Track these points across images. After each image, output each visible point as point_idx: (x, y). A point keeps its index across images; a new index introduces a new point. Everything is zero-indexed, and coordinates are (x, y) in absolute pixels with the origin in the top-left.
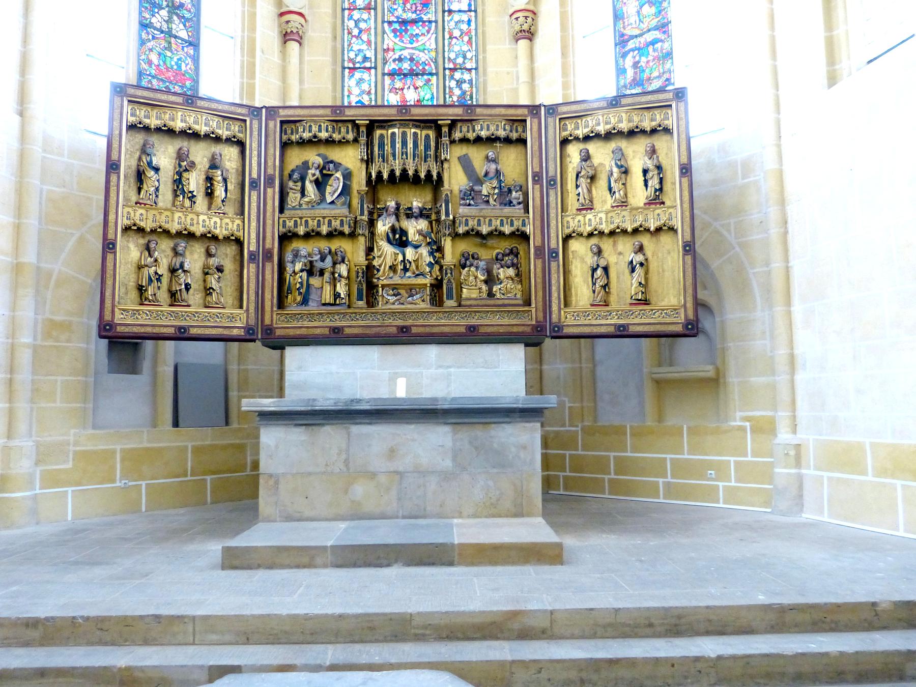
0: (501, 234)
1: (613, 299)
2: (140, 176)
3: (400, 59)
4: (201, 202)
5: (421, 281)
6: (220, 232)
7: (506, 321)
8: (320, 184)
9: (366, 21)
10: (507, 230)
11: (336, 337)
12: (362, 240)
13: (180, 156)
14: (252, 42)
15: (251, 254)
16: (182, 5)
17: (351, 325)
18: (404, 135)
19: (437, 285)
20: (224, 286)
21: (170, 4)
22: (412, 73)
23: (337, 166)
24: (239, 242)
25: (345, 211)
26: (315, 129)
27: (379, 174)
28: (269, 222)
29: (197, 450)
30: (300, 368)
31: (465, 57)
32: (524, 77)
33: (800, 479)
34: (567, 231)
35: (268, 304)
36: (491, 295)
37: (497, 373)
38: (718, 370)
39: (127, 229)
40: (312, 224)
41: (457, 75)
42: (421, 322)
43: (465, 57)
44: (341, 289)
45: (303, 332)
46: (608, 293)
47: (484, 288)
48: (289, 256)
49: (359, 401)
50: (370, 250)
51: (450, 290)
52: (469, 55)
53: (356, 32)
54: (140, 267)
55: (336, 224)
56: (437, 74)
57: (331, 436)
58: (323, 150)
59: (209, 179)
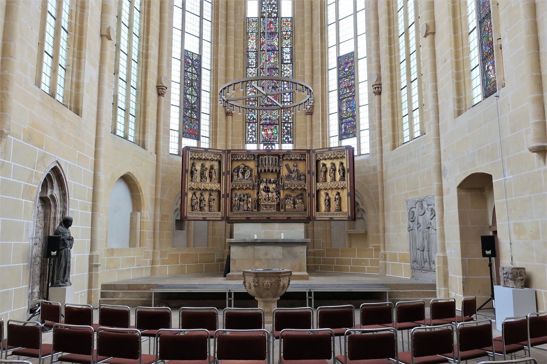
0: (298, 189)
1: (331, 209)
2: (192, 173)
3: (266, 119)
4: (208, 179)
5: (273, 203)
6: (214, 189)
7: (299, 216)
8: (243, 174)
10: (299, 188)
11: (248, 220)
12: (256, 190)
13: (203, 166)
14: (216, 116)
15: (223, 195)
16: (195, 107)
17: (252, 217)
18: (269, 158)
19: (278, 204)
20: (214, 204)
22: (270, 124)
23: (248, 167)
24: (219, 192)
25: (250, 182)
26: (242, 156)
27: (261, 170)
28: (228, 185)
29: (201, 255)
30: (238, 230)
31: (289, 118)
32: (309, 128)
33: (385, 264)
34: (318, 188)
35: (228, 210)
36: (294, 208)
37: (296, 232)
38: (366, 231)
39: (190, 188)
40: (241, 186)
41: (286, 125)
42: (273, 216)
43: (289, 118)
44: (249, 205)
45: (238, 218)
46: (330, 207)
47: (292, 205)
48: (234, 195)
50: (258, 193)
51: (282, 207)
52: (290, 118)
54: (192, 200)
55: (248, 186)
56: (279, 125)
57: (250, 249)
58: (244, 162)
59: (210, 172)
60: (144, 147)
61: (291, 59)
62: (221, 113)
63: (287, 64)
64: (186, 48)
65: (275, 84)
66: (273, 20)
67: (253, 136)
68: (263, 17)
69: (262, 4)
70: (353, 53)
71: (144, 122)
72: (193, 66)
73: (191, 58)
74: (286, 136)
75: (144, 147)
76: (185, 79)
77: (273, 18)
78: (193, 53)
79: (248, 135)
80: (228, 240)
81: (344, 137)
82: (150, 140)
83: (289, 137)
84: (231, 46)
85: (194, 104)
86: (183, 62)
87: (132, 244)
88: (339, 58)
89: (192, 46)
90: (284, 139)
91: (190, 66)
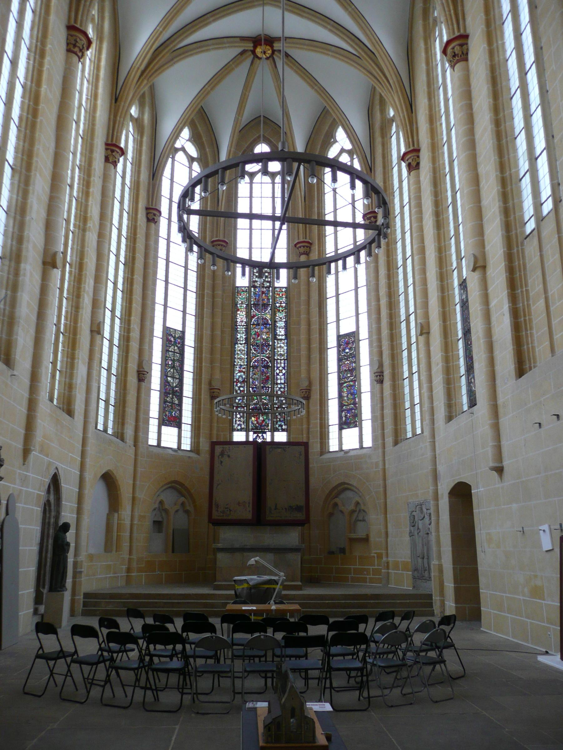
9: (242, 387)
16: (176, 391)
33: (388, 573)
49: (247, 545)
53: (239, 392)
60: (122, 439)
61: (286, 335)
62: (205, 396)
63: (281, 340)
64: (168, 325)
65: (268, 363)
66: (265, 289)
67: (242, 423)
68: (255, 287)
69: (253, 272)
70: (354, 332)
71: (124, 411)
72: (175, 344)
73: (173, 335)
74: (279, 423)
75: (122, 439)
77: (266, 287)
78: (175, 330)
79: (236, 421)
80: (214, 546)
81: (345, 427)
82: (129, 432)
83: (283, 424)
84: (218, 320)
85: (176, 387)
86: (165, 340)
87: (108, 547)
88: (339, 337)
89: (175, 323)
90: (277, 426)
91: (172, 345)
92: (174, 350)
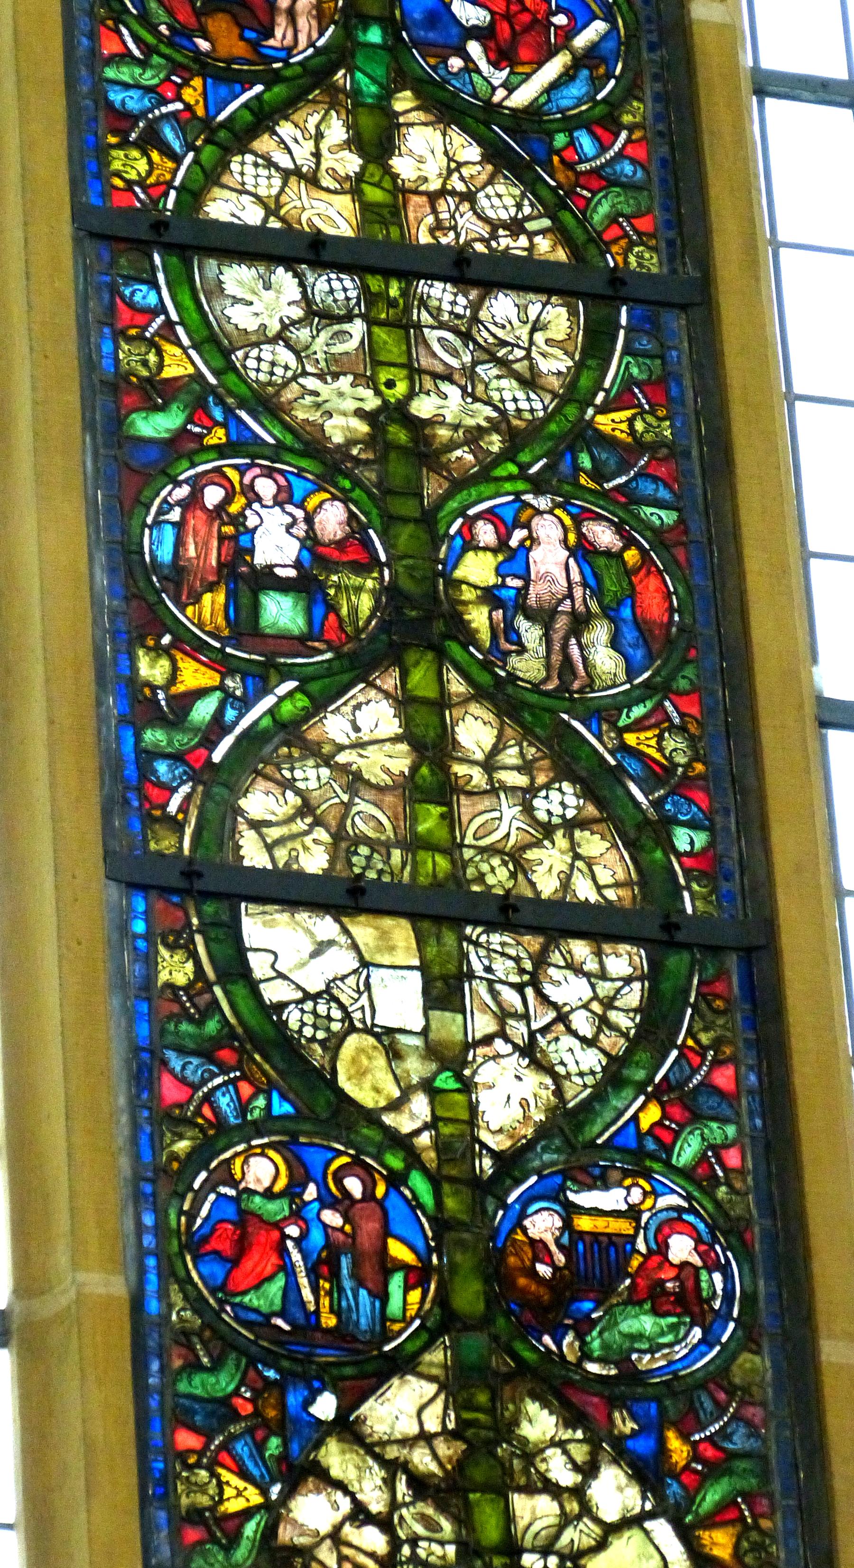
16: (599, 1267)
21: (469, 1296)
76: (126, 475)
85: (569, 1143)
91: (313, 82)
92: (385, 204)
